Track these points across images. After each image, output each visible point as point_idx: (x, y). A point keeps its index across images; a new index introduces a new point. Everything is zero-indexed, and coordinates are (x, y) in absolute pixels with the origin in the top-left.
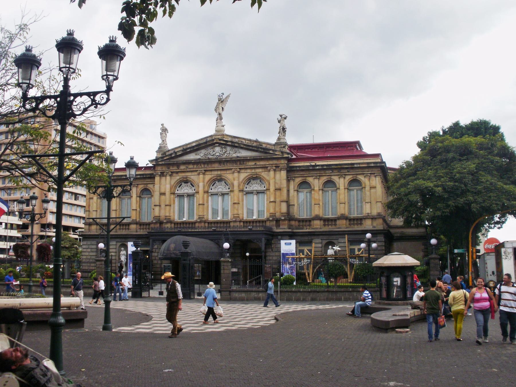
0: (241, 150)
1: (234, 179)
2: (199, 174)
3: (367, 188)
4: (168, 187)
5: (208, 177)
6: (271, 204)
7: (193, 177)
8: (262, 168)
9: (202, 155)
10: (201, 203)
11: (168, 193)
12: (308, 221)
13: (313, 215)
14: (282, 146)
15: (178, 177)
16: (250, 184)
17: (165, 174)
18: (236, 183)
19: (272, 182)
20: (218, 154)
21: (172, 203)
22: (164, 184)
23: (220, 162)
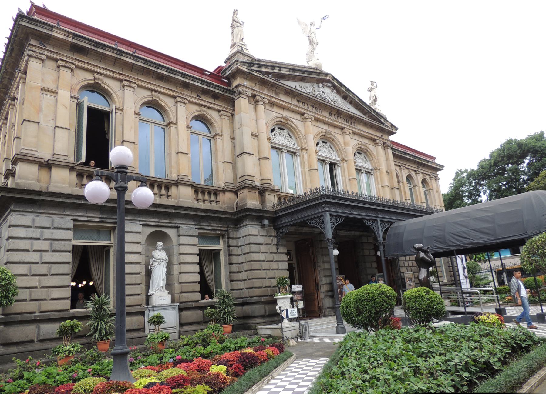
3: (435, 191)
4: (263, 123)
22: (253, 118)
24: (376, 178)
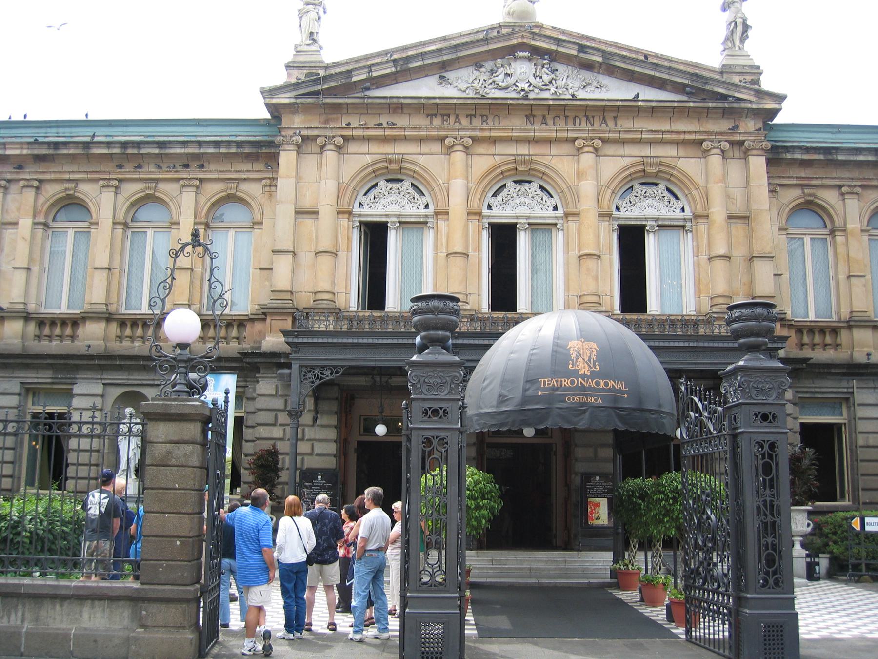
0: (606, 80)
1: (579, 175)
2: (449, 150)
4: (329, 186)
5: (482, 162)
6: (719, 264)
7: (427, 160)
8: (676, 143)
9: (463, 86)
10: (458, 248)
11: (327, 211)
12: (828, 331)
13: (845, 314)
14: (749, 78)
15: (369, 159)
16: (631, 196)
17: (320, 141)
18: (588, 188)
19: (716, 192)
20: (526, 87)
21: (342, 246)
23: (531, 110)
24: (697, 239)
